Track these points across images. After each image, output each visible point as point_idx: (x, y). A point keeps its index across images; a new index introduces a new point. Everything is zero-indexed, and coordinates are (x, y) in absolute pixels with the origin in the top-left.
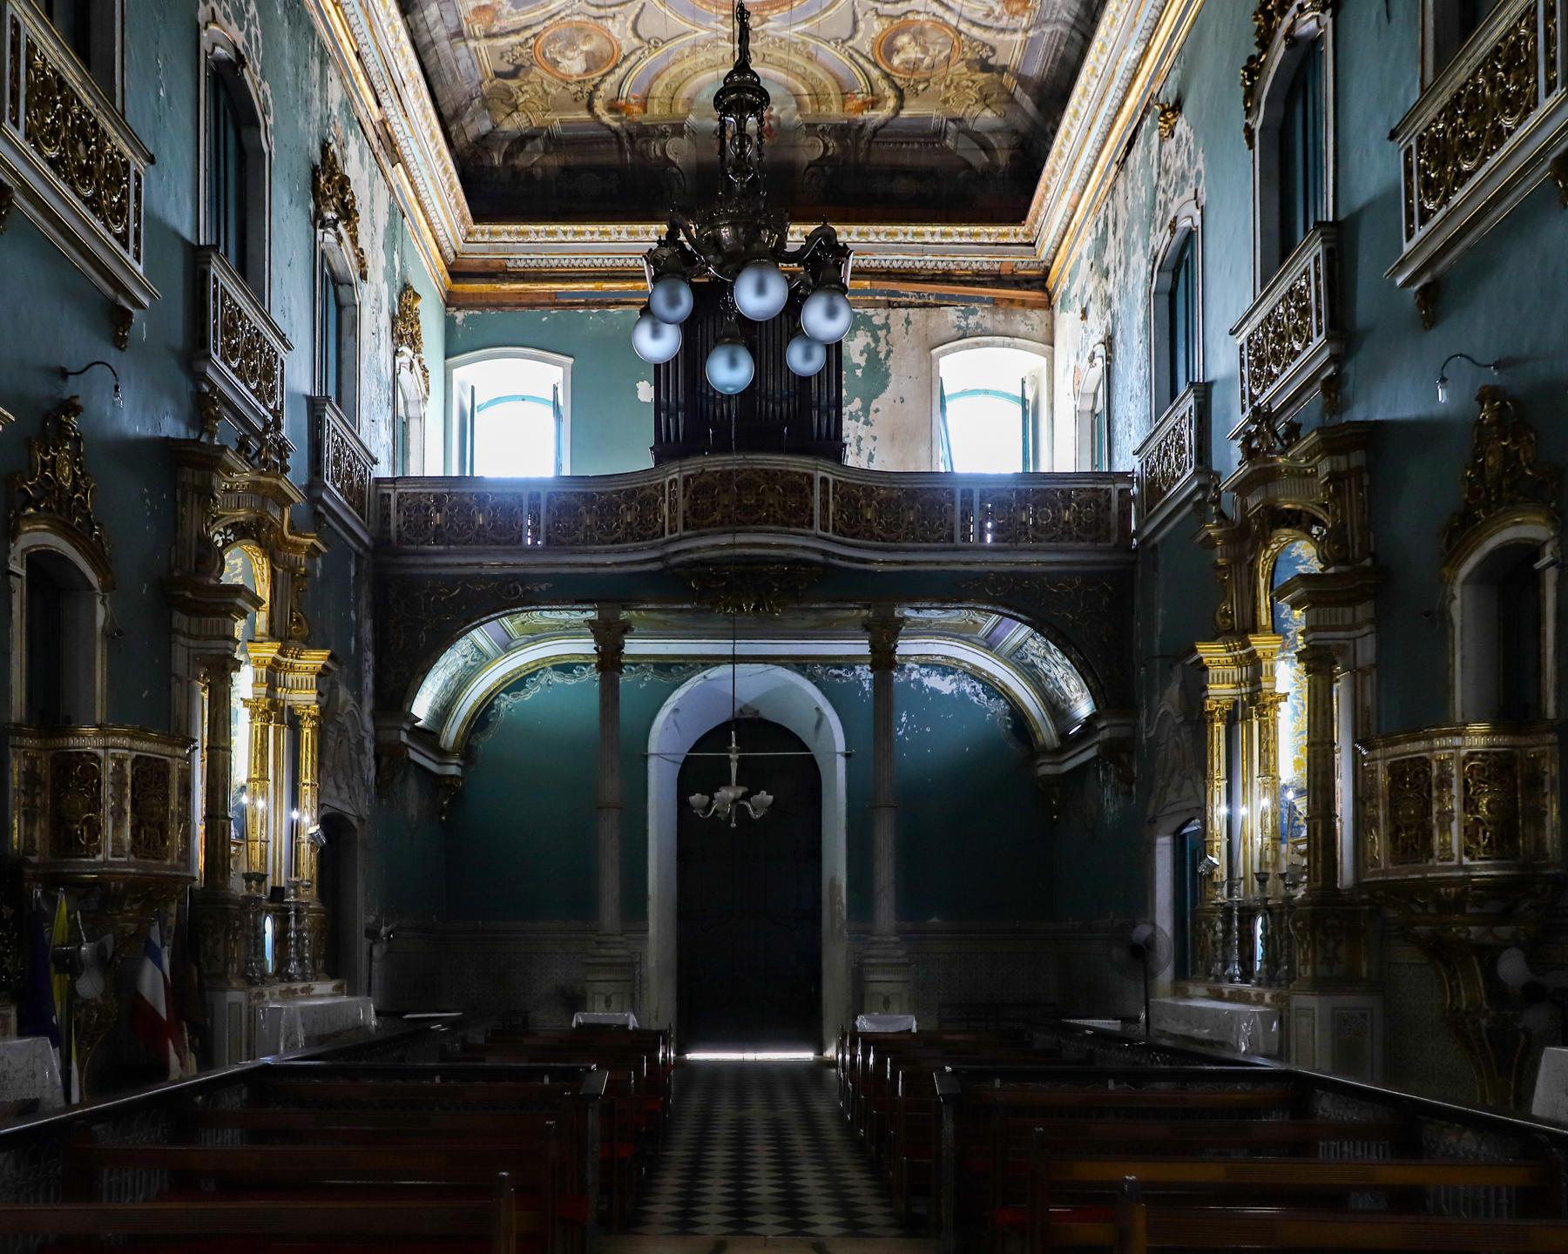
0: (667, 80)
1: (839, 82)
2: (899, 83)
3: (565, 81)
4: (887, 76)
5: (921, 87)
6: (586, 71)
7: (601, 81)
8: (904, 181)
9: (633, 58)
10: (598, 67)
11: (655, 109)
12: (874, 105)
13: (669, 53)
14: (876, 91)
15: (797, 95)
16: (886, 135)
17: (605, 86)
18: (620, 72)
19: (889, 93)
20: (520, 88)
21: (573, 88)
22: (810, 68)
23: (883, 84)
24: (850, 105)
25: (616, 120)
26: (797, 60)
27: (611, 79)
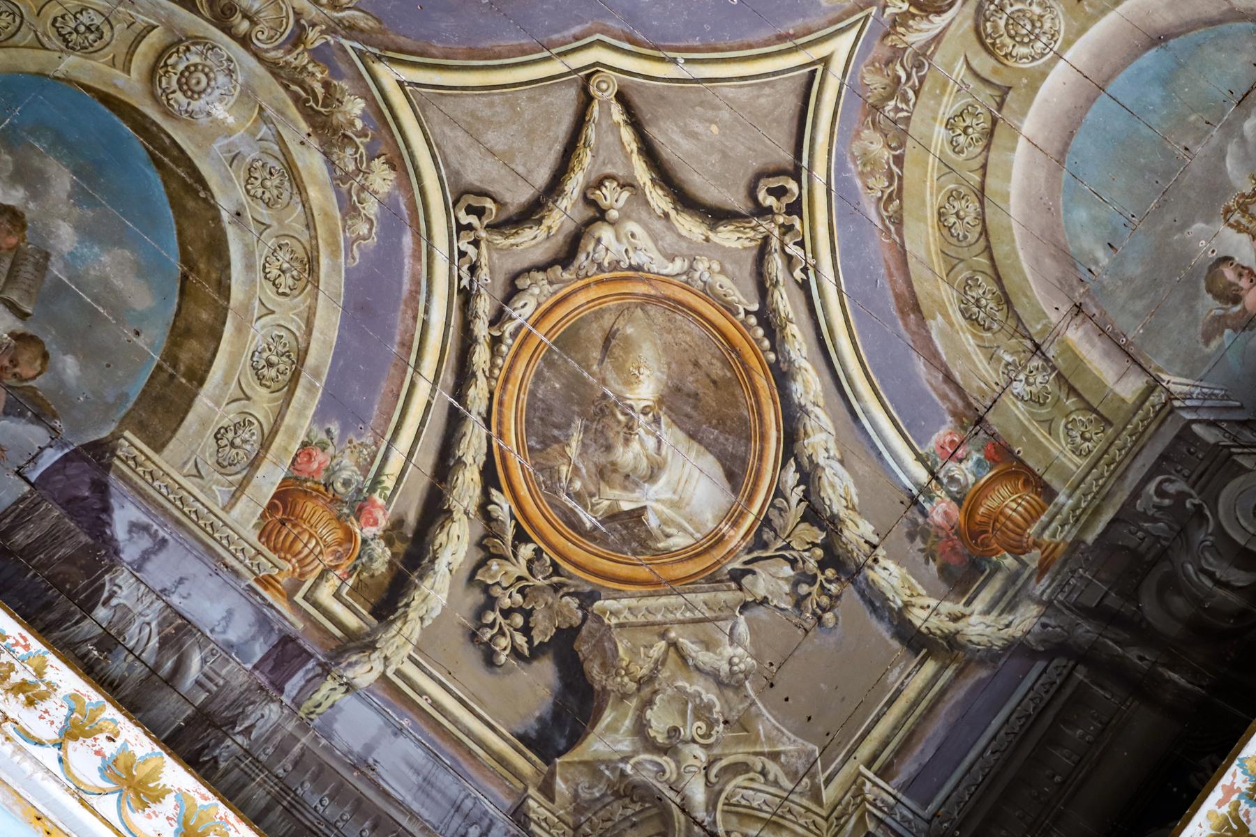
0: (947, 294)
6: (735, 473)
7: (809, 477)
9: (785, 302)
10: (747, 432)
11: (1062, 452)
13: (842, 194)
17: (838, 488)
18: (809, 385)
20: (641, 727)
25: (1007, 603)
27: (820, 439)
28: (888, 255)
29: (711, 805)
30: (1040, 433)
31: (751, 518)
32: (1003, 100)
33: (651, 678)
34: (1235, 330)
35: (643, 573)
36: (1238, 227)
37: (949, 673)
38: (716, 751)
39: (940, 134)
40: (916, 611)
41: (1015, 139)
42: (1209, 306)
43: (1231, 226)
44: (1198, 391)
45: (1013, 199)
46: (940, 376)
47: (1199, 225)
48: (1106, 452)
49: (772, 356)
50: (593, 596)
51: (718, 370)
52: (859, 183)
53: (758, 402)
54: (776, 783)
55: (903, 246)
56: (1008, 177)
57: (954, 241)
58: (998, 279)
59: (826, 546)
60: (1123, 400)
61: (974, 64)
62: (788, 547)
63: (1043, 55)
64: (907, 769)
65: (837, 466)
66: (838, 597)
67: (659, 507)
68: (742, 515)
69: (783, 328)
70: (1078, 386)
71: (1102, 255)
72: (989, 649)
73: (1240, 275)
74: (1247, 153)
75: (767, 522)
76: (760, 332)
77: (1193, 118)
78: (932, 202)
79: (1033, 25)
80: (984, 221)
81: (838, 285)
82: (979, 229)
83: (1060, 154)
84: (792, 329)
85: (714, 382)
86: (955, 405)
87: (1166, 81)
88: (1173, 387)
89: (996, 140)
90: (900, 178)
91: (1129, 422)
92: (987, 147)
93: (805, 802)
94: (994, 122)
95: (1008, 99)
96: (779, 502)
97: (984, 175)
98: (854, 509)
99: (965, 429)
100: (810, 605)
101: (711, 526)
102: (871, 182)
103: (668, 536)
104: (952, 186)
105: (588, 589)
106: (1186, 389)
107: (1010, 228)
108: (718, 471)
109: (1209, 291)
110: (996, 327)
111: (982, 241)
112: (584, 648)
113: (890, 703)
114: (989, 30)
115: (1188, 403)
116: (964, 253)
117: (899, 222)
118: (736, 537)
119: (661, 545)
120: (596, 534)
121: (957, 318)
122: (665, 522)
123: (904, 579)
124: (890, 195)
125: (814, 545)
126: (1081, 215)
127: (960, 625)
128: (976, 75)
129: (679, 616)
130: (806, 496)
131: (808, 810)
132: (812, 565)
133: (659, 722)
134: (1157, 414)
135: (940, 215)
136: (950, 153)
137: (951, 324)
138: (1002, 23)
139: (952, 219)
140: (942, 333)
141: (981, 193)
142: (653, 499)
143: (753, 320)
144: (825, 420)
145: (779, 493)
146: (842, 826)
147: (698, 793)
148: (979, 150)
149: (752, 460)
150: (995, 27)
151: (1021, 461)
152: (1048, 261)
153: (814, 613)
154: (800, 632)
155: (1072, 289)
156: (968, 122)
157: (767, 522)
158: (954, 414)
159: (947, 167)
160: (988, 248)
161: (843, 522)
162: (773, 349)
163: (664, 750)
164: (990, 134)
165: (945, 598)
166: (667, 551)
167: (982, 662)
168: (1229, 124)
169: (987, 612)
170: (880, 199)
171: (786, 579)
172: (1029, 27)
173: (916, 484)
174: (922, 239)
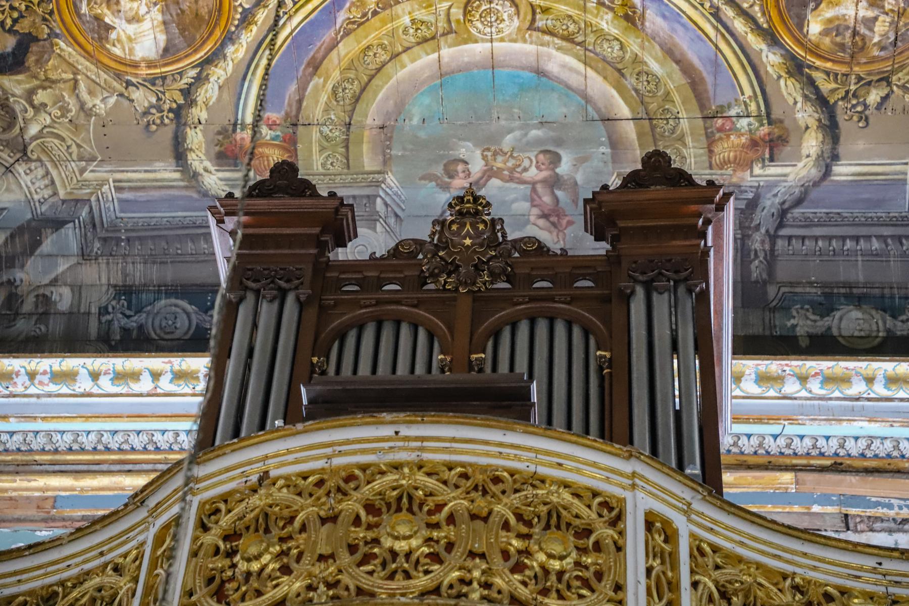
0: (336, 75)
1: (695, 83)
2: (826, 86)
3: (123, 71)
4: (796, 68)
5: (874, 97)
7: (200, 80)
8: (856, 314)
12: (774, 143)
14: (776, 113)
15: (608, 120)
16: (808, 223)
19: (806, 115)
21: (142, 97)
22: (634, 45)
23: (789, 90)
24: (725, 149)
26: (606, 22)
27: (219, 73)
28: (328, 40)
29: (35, 138)
30: (315, 148)
31: (158, 71)
32: (447, 34)
33: (54, 82)
34: (437, 185)
35: (90, 48)
36: (484, 158)
37: (182, 184)
38: (56, 126)
39: (406, 20)
40: (194, 155)
41: (434, 52)
42: (439, 170)
43: (482, 155)
44: (396, 189)
45: (405, 70)
46: (297, 98)
47: (470, 144)
48: (335, 175)
49: (233, 29)
50: (57, 36)
51: (204, 12)
52: (348, 5)
53: (208, 38)
54: (70, 154)
55: (338, 43)
56: (413, 61)
57: (362, 61)
58: (363, 90)
59: (180, 107)
60: (364, 167)
61: (453, 10)
62: (164, 93)
63: (485, 35)
64: (126, 195)
65: (216, 87)
66: (165, 125)
67: (122, 33)
68: (155, 67)
69: (250, 24)
70: (351, 148)
71: (416, 121)
72: (207, 191)
73: (464, 172)
74: (520, 140)
75: (164, 78)
76: (238, 16)
77: (516, 110)
78: (371, 38)
79: (496, 20)
80: (384, 66)
81: (293, 31)
82: (378, 66)
83: (443, 74)
84: (254, 29)
85: (197, 14)
86: (291, 111)
87: (523, 88)
88: (388, 180)
89: (425, 45)
90: (368, 20)
91: (357, 174)
92: (418, 44)
93: (75, 169)
94: (433, 38)
95: (450, 36)
96: (178, 77)
97: (404, 51)
98: (206, 105)
99: (285, 121)
100: (150, 117)
101: (137, 59)
102: (353, 9)
103: (114, 45)
104: (386, 42)
105: (58, 31)
106: (393, 185)
107: (391, 78)
108: (162, 45)
109: (445, 165)
110: (342, 103)
111: (374, 72)
112: (34, 48)
113: (146, 171)
114: (475, 5)
115: (387, 190)
116: (361, 69)
117: (347, 34)
118: (144, 71)
119: (108, 46)
120: (84, 18)
121: (329, 86)
122: (119, 40)
123: (200, 142)
124: (355, 22)
125: (175, 101)
126: (427, 100)
127: (205, 174)
128: (448, 14)
129: (89, 74)
130: (191, 85)
131: (74, 172)
132: (166, 107)
133: (41, 97)
134: (371, 182)
135: (368, 47)
136: (401, 31)
137: (324, 86)
138: (484, 8)
139: (371, 54)
140: (316, 86)
141: (395, 56)
142: (122, 29)
143: (240, 10)
144: (230, 69)
145: (181, 74)
146: (81, 189)
147: (33, 130)
148: (414, 41)
149: (182, 54)
150: (479, 6)
151: (296, 150)
152: (391, 102)
153: (148, 122)
154: (135, 122)
155: (389, 119)
156: (422, 28)
157: (164, 78)
158: (287, 115)
159: (393, 33)
160: (372, 77)
161: (196, 105)
162: (237, 27)
163: (33, 107)
164: (426, 40)
165: (210, 161)
166: (108, 51)
167: (199, 192)
168: (528, 125)
169: (221, 180)
170: (349, 19)
171: (149, 102)
172: (493, 19)
173: (243, 120)
174: (347, 49)
